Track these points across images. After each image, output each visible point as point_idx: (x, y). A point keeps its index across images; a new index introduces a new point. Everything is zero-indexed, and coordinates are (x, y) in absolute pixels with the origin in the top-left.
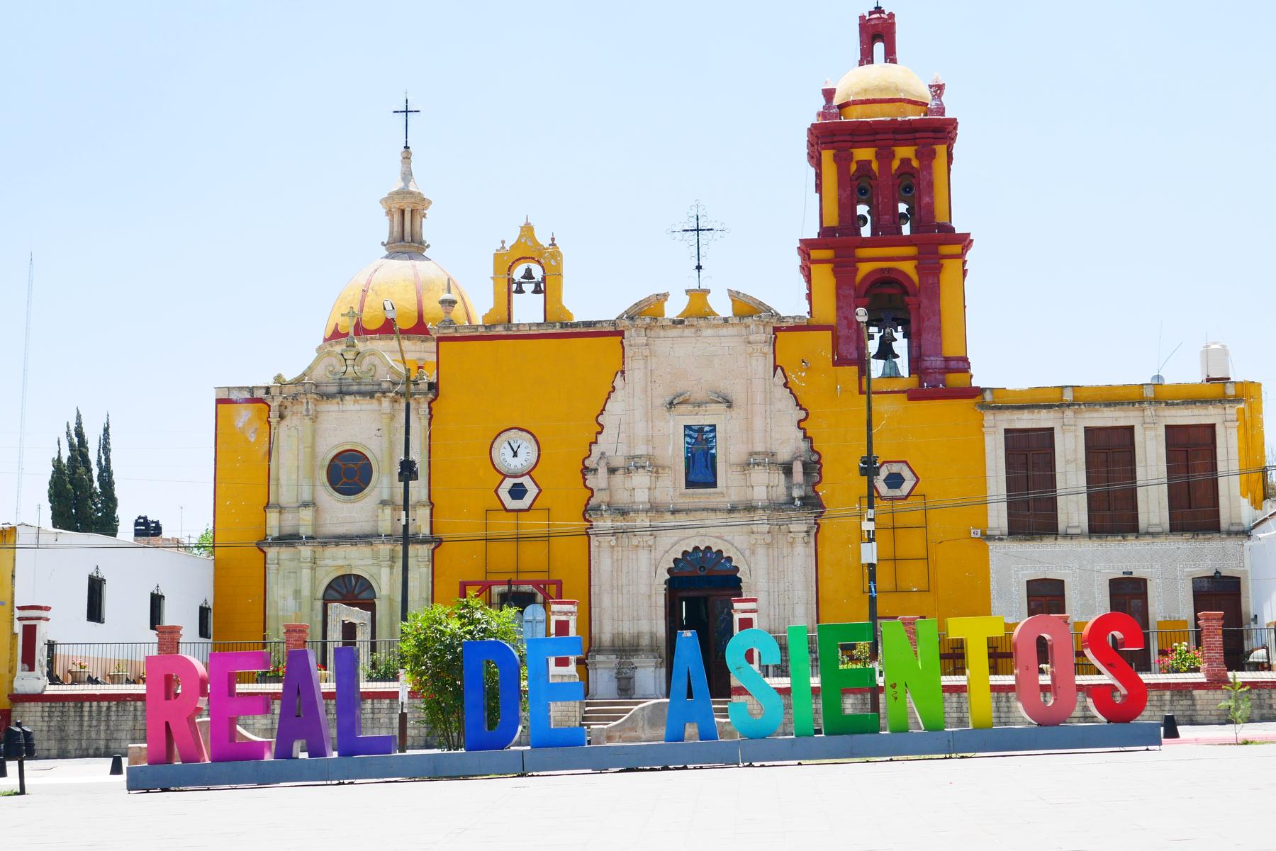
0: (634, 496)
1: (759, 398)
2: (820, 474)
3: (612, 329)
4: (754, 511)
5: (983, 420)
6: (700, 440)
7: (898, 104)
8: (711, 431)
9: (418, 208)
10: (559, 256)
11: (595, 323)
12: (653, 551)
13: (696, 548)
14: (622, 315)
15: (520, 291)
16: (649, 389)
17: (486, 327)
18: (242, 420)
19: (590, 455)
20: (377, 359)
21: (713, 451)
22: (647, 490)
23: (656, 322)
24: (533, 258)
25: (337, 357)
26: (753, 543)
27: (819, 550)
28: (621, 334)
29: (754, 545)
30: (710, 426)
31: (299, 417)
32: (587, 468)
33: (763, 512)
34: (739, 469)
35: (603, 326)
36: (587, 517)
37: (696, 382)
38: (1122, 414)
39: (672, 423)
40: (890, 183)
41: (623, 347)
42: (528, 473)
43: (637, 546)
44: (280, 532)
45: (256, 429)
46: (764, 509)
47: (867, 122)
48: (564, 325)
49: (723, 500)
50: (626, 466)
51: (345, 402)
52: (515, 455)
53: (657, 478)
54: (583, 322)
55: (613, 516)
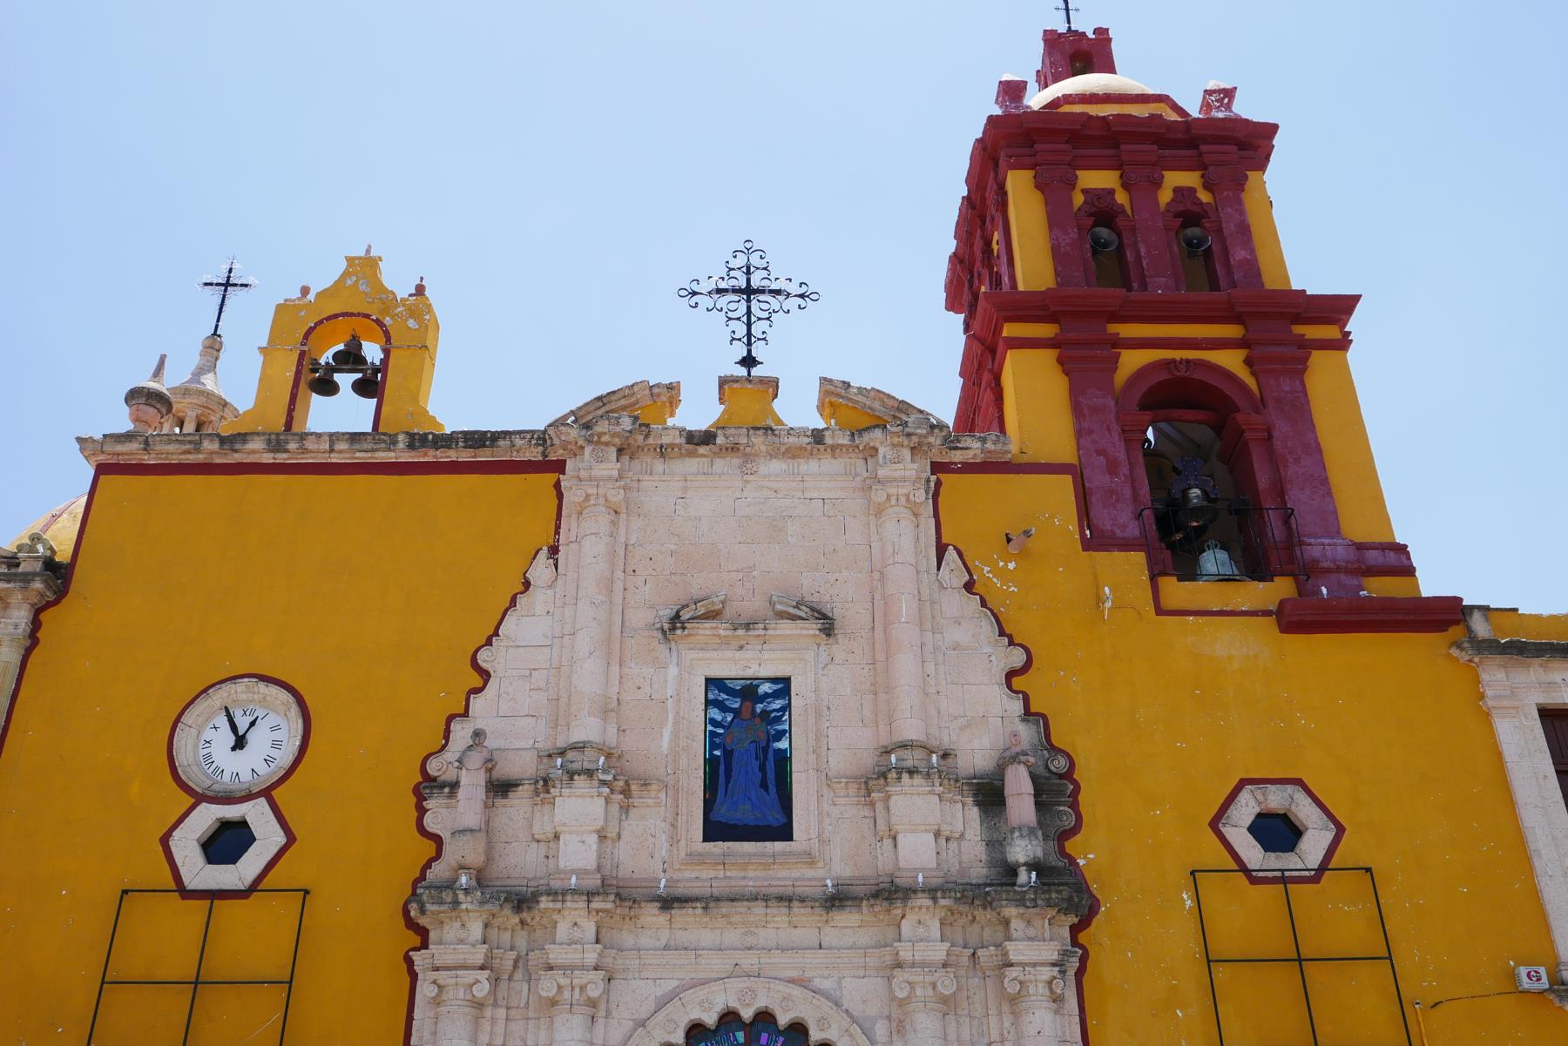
0: (556, 857)
1: (905, 608)
2: (1075, 805)
3: (534, 454)
4: (906, 899)
5: (1478, 681)
6: (746, 715)
8: (776, 695)
9: (212, 418)
10: (428, 313)
11: (496, 437)
12: (601, 1021)
13: (729, 1018)
14: (566, 417)
15: (327, 387)
16: (618, 586)
17: (223, 440)
19: (443, 748)
21: (783, 744)
22: (595, 837)
23: (647, 436)
26: (901, 994)
27: (1092, 1023)
28: (559, 466)
29: (902, 1003)
30: (774, 680)
32: (434, 779)
33: (929, 902)
34: (853, 789)
36: (413, 914)
37: (741, 575)
39: (673, 671)
40: (1160, 224)
41: (560, 496)
42: (267, 793)
43: (553, 1003)
46: (933, 892)
48: (417, 441)
49: (810, 873)
50: (542, 774)
52: (240, 743)
53: (625, 809)
54: (465, 433)
55: (488, 907)
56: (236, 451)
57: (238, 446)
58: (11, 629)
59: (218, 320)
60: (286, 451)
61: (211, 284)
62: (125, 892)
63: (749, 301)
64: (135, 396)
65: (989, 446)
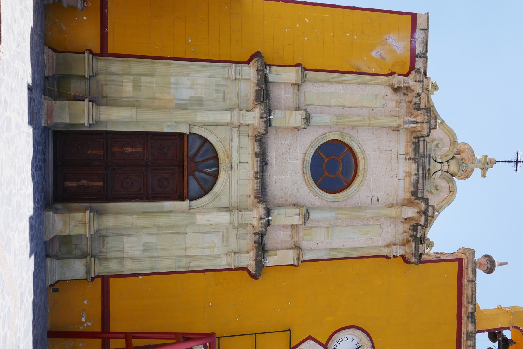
17: (473, 313)
20: (446, 196)
31: (395, 109)
44: (272, 82)
45: (383, 59)
51: (408, 162)
56: (468, 318)
57: (470, 320)
58: (395, 251)
59: (502, 162)
60: (467, 339)
61: (517, 156)
62: (289, 330)
64: (492, 263)
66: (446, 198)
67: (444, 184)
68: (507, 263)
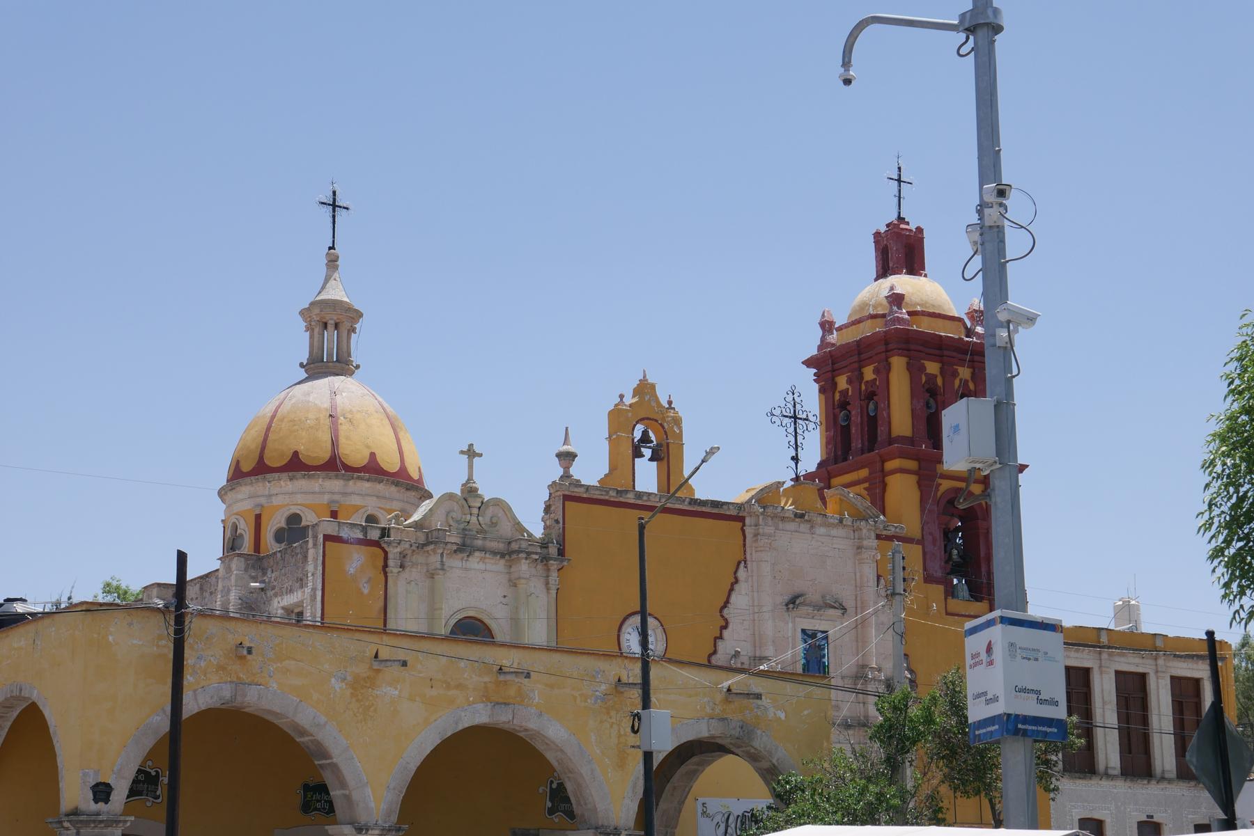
3: (733, 512)
7: (956, 323)
8: (823, 639)
17: (618, 492)
18: (354, 565)
20: (501, 510)
24: (656, 421)
25: (460, 503)
35: (729, 509)
37: (811, 583)
38: (1137, 660)
39: (790, 625)
47: (941, 336)
48: (695, 502)
51: (470, 559)
56: (621, 497)
58: (553, 582)
59: (334, 237)
63: (791, 417)
65: (897, 530)
66: (504, 510)
67: (490, 512)
68: (567, 429)
